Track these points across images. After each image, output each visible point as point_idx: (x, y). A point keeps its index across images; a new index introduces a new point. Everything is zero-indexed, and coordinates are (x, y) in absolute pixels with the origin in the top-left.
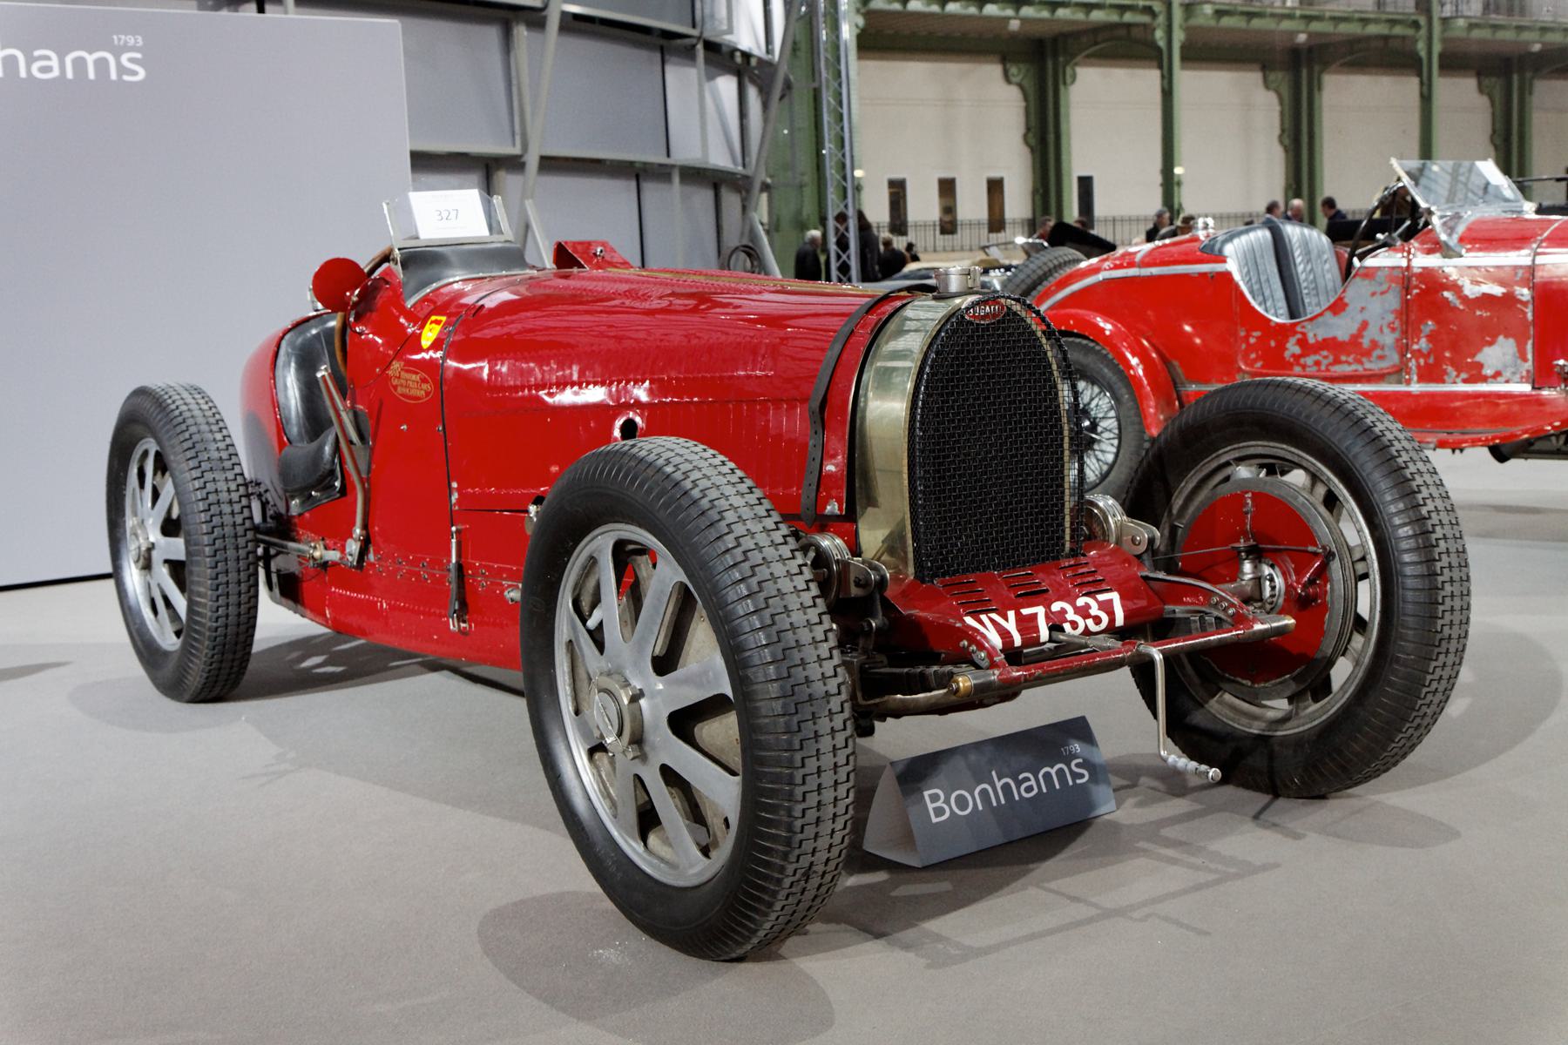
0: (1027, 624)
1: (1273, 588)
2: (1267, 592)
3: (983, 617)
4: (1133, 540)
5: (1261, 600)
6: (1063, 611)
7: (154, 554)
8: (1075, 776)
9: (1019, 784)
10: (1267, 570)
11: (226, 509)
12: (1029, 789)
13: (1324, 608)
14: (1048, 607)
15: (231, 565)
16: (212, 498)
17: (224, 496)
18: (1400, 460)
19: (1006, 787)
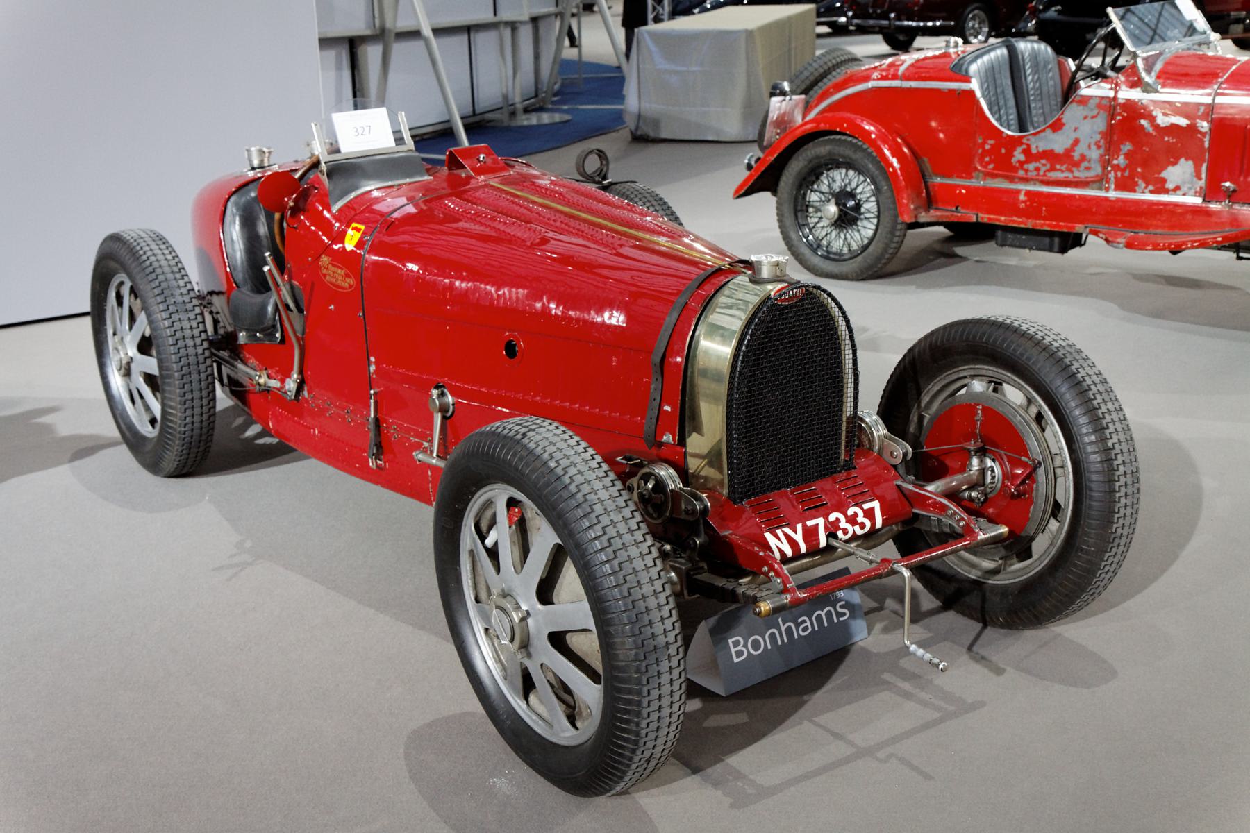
0: (810, 534)
1: (993, 477)
2: (989, 480)
3: (779, 532)
4: (892, 453)
5: (984, 485)
6: (838, 520)
7: (133, 366)
8: (839, 615)
9: (798, 626)
10: (989, 463)
11: (190, 343)
12: (805, 629)
13: (1030, 501)
14: (826, 517)
15: (195, 386)
16: (179, 335)
17: (188, 333)
18: (1095, 402)
19: (789, 630)
